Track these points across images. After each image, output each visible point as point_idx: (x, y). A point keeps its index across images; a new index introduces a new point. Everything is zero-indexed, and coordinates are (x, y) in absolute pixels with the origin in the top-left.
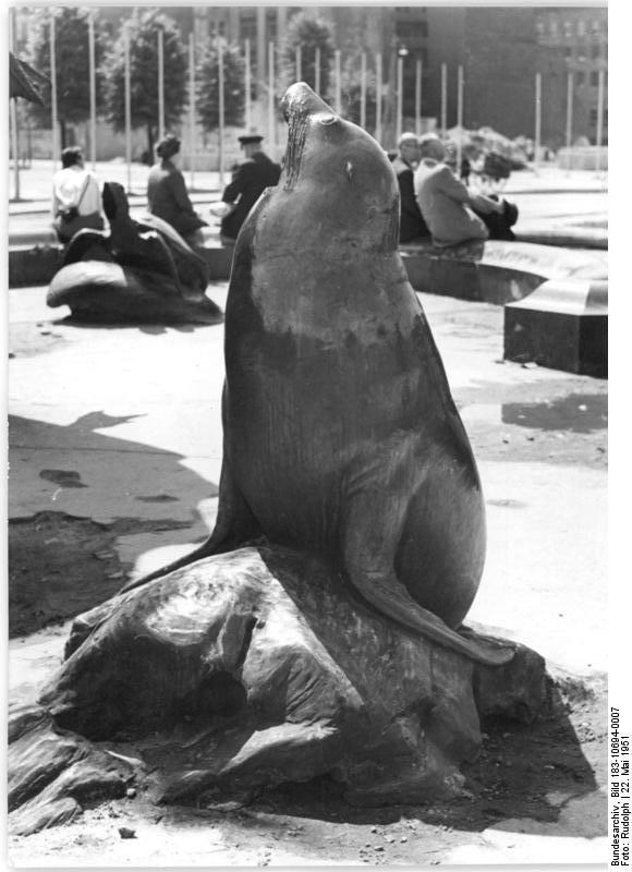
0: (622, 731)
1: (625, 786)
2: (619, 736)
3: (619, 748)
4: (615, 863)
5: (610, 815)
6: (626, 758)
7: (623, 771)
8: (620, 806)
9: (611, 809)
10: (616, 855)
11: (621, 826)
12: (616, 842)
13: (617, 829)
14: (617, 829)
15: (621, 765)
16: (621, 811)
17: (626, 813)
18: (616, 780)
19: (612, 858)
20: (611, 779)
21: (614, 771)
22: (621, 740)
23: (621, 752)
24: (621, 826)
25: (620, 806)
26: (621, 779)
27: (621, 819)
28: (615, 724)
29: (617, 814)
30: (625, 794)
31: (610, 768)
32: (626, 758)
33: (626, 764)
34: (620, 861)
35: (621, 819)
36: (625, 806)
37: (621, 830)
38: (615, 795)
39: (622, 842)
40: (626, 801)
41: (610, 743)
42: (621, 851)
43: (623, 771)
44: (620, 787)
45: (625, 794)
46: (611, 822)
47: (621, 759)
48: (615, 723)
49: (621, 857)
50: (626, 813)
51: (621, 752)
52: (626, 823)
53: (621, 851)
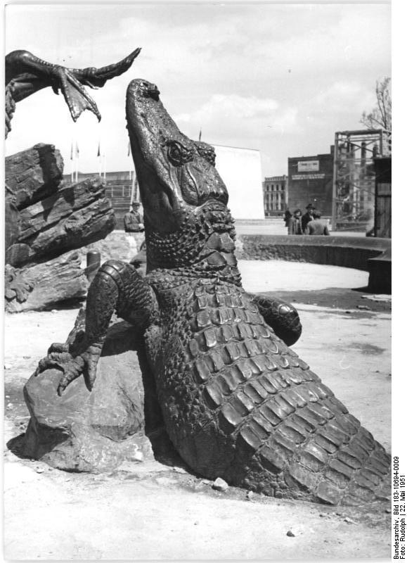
1: (402, 508)
2: (398, 475)
3: (400, 482)
4: (396, 558)
5: (393, 526)
6: (403, 489)
8: (399, 520)
9: (393, 522)
11: (400, 533)
12: (397, 543)
13: (397, 536)
14: (397, 536)
15: (400, 494)
16: (400, 524)
17: (403, 525)
18: (396, 503)
19: (393, 554)
20: (393, 503)
22: (400, 478)
23: (400, 485)
24: (400, 533)
25: (399, 520)
27: (400, 529)
29: (397, 525)
30: (403, 512)
31: (393, 496)
32: (403, 489)
35: (400, 529)
37: (400, 536)
38: (396, 513)
39: (401, 544)
40: (403, 517)
41: (393, 480)
42: (400, 549)
44: (399, 508)
45: (403, 512)
46: (393, 530)
47: (400, 490)
48: (396, 467)
49: (400, 553)
51: (400, 485)
53: (400, 549)
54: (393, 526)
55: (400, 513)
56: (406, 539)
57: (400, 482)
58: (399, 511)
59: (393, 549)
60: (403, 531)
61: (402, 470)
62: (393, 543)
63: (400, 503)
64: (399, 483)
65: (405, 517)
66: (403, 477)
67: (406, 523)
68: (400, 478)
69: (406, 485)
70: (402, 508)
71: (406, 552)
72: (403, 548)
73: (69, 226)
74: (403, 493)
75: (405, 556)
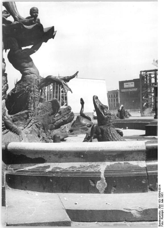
1: (162, 206)
2: (161, 192)
4: (160, 226)
7: (162, 202)
9: (158, 211)
11: (161, 216)
12: (160, 220)
13: (160, 217)
14: (160, 217)
16: (161, 212)
17: (162, 213)
18: (160, 204)
19: (159, 224)
21: (159, 201)
22: (161, 193)
23: (161, 197)
24: (161, 216)
25: (161, 211)
27: (161, 214)
29: (160, 213)
30: (162, 208)
34: (161, 225)
37: (161, 217)
38: (160, 208)
40: (162, 209)
42: (161, 223)
43: (162, 202)
44: (161, 206)
45: (162, 208)
47: (161, 198)
48: (160, 189)
49: (161, 224)
51: (161, 197)
53: (161, 223)
54: (158, 213)
56: (163, 218)
60: (162, 215)
61: (162, 191)
63: (161, 204)
64: (161, 196)
65: (163, 209)
67: (163, 212)
68: (161, 193)
69: (163, 196)
71: (163, 224)
72: (162, 222)
73: (64, 119)
74: (162, 200)
75: (163, 225)
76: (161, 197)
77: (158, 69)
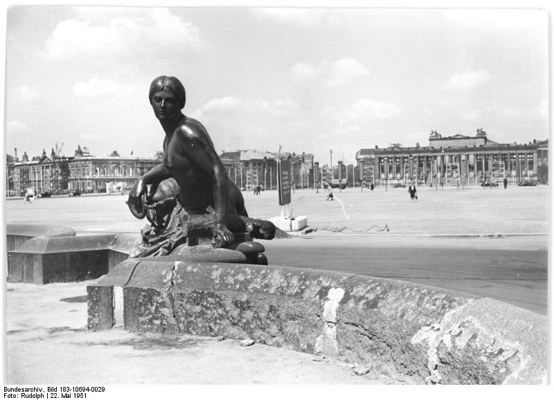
0: (89, 394)
1: (54, 396)
2: (86, 392)
3: (79, 392)
4: (5, 389)
6: (73, 396)
7: (64, 394)
8: (42, 392)
10: (11, 390)
11: (29, 393)
12: (19, 390)
13: (27, 390)
14: (27, 390)
16: (39, 393)
17: (38, 396)
18: (59, 389)
19: (9, 387)
22: (84, 393)
23: (76, 393)
24: (29, 393)
25: (42, 392)
26: (59, 393)
27: (34, 393)
28: (94, 389)
29: (37, 390)
32: (73, 396)
33: (69, 396)
36: (42, 396)
37: (26, 393)
38: (49, 389)
40: (45, 396)
42: (13, 393)
43: (64, 394)
44: (54, 392)
45: (50, 396)
47: (72, 393)
48: (95, 389)
49: (10, 393)
50: (38, 396)
51: (76, 393)
52: (31, 396)
53: (13, 393)
55: (49, 393)
57: (80, 393)
58: (51, 392)
59: (14, 387)
62: (20, 387)
66: (84, 396)
68: (84, 393)
70: (54, 396)
76: (75, 392)
77: (543, 254)
